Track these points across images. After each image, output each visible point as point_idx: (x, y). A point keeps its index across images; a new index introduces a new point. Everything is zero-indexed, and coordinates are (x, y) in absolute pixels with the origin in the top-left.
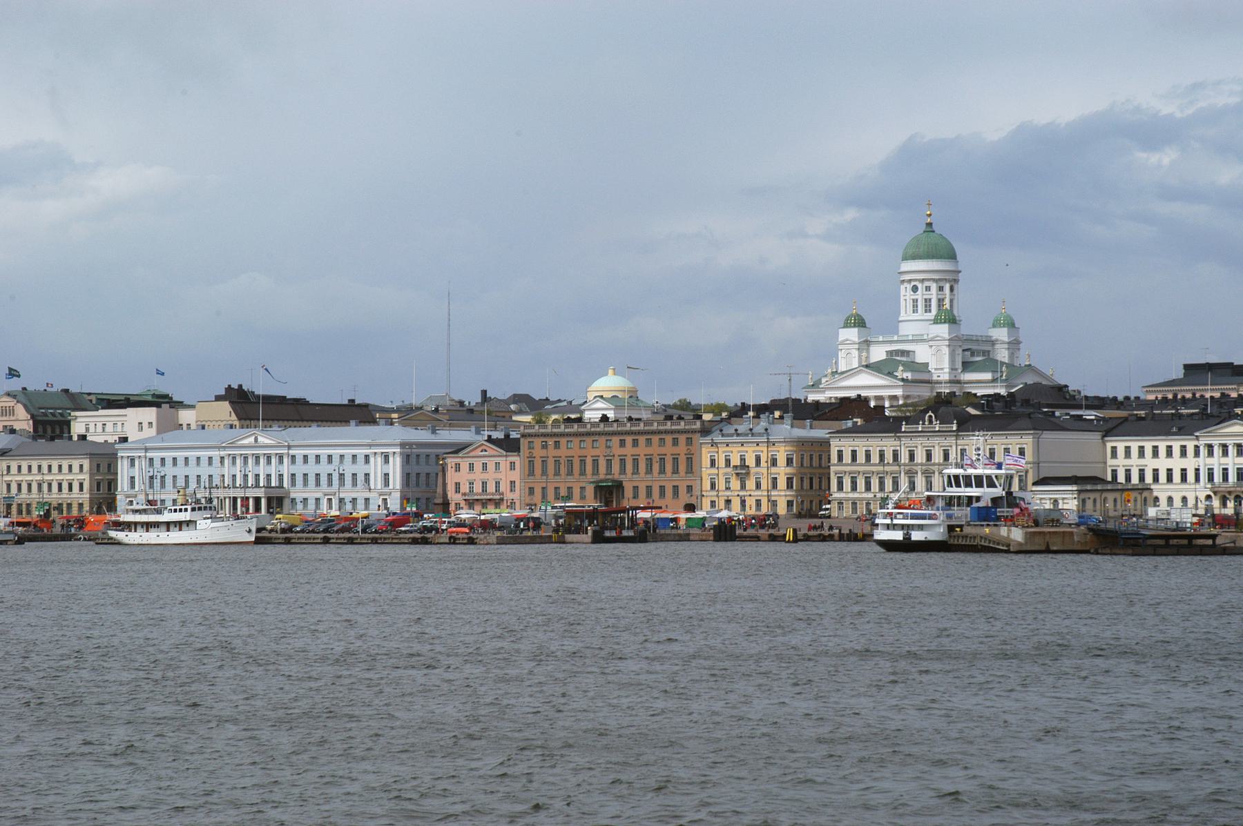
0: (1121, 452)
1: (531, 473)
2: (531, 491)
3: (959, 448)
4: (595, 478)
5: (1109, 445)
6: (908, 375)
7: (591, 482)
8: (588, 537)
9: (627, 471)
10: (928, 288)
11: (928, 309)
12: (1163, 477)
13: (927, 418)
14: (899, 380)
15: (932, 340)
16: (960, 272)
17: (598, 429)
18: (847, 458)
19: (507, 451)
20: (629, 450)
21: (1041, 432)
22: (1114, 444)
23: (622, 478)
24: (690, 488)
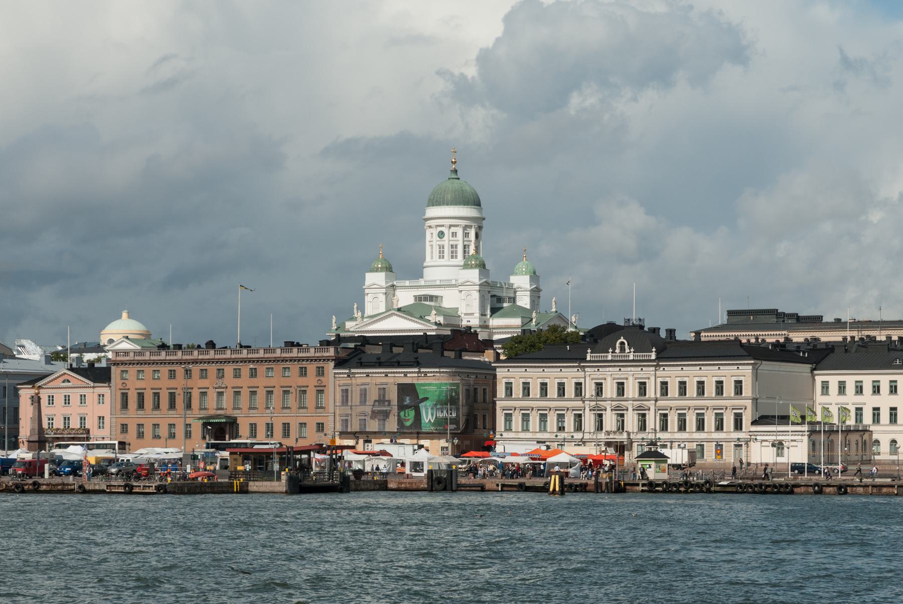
0: (834, 388)
1: (125, 405)
3: (659, 380)
4: (204, 414)
5: (819, 379)
6: (441, 319)
7: (200, 418)
8: (281, 485)
10: (454, 234)
11: (453, 256)
12: (885, 416)
13: (618, 345)
14: (432, 323)
17: (207, 357)
18: (518, 391)
19: (94, 382)
20: (245, 381)
21: (759, 362)
22: (825, 378)
23: (236, 413)
24: (320, 427)
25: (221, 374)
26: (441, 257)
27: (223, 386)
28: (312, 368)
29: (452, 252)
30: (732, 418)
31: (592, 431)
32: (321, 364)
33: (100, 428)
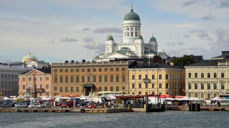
2: (56, 89)
4: (83, 83)
6: (130, 55)
7: (82, 85)
8: (144, 109)
9: (97, 81)
10: (132, 29)
15: (136, 44)
16: (141, 24)
18: (193, 76)
19: (45, 73)
20: (97, 73)
23: (94, 83)
25: (89, 70)
26: (128, 35)
27: (90, 74)
28: (120, 68)
29: (132, 34)
30: (213, 85)
31: (220, 89)
32: (124, 67)
33: (23, 89)
